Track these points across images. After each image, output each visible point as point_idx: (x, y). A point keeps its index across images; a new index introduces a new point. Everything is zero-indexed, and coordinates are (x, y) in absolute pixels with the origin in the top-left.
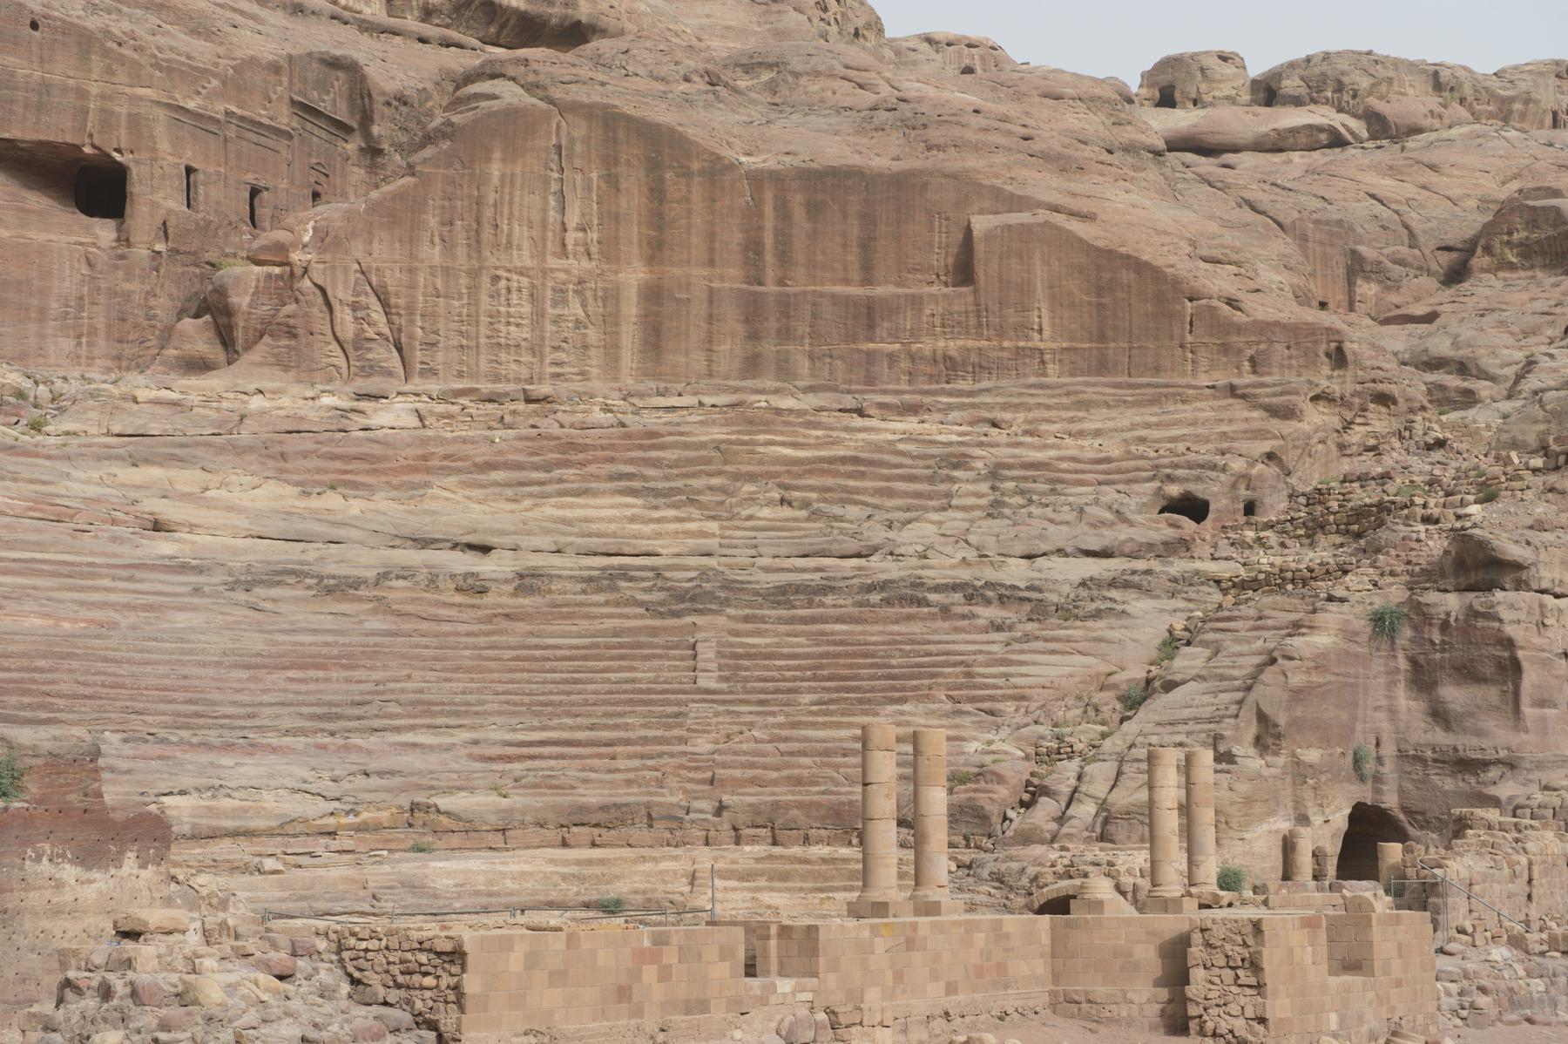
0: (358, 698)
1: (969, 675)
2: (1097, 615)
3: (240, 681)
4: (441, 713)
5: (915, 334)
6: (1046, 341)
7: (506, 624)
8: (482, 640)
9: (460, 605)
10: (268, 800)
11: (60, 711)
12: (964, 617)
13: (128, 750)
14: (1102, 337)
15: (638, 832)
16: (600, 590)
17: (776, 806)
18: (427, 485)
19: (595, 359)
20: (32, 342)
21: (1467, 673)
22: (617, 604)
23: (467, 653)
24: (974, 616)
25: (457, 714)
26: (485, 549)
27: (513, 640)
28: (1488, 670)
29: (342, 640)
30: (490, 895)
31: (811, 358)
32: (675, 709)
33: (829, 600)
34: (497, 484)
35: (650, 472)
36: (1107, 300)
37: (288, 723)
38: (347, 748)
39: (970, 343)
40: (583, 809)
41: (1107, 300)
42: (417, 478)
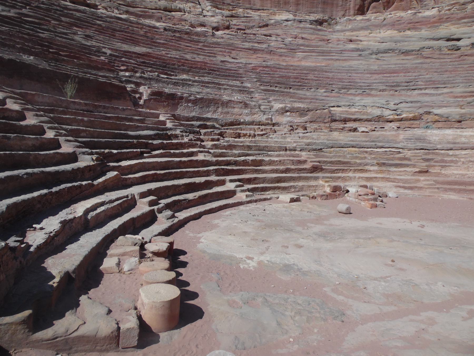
0: (408, 81)
3: (368, 77)
4: (438, 84)
7: (466, 57)
8: (456, 63)
9: (448, 54)
10: (369, 110)
11: (305, 83)
13: (325, 94)
18: (440, 25)
20: (334, 13)
23: (450, 67)
25: (444, 84)
26: (458, 40)
27: (469, 62)
29: (404, 66)
30: (455, 143)
34: (465, 23)
37: (381, 88)
38: (401, 95)
42: (436, 24)
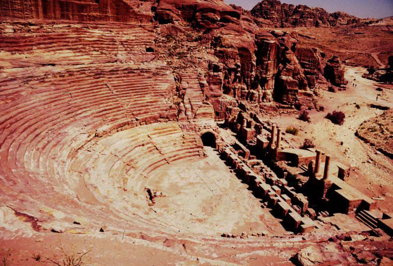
1: (153, 88)
2: (163, 75)
5: (90, 12)
6: (109, 15)
12: (142, 75)
14: (117, 14)
15: (127, 126)
16: (82, 74)
17: (146, 118)
19: (34, 14)
21: (215, 84)
22: (87, 77)
24: (144, 75)
28: (217, 83)
31: (73, 15)
32: (115, 100)
33: (119, 72)
34: (43, 48)
35: (70, 44)
36: (118, 8)
39: (98, 14)
40: (120, 124)
41: (118, 8)
